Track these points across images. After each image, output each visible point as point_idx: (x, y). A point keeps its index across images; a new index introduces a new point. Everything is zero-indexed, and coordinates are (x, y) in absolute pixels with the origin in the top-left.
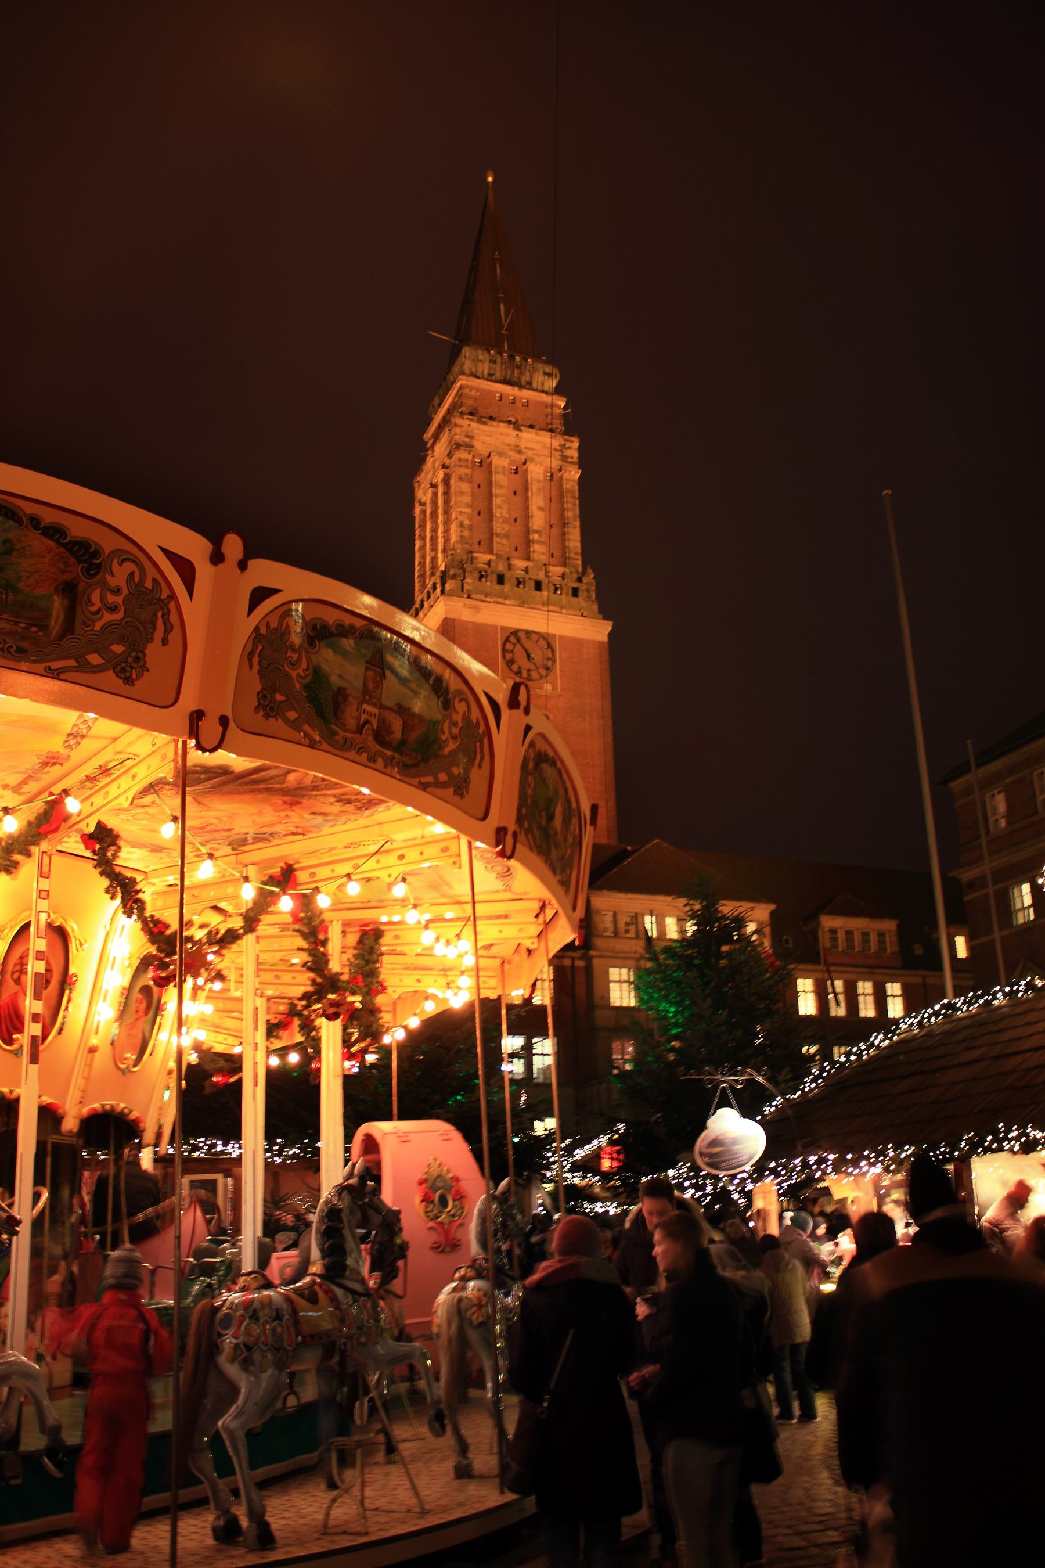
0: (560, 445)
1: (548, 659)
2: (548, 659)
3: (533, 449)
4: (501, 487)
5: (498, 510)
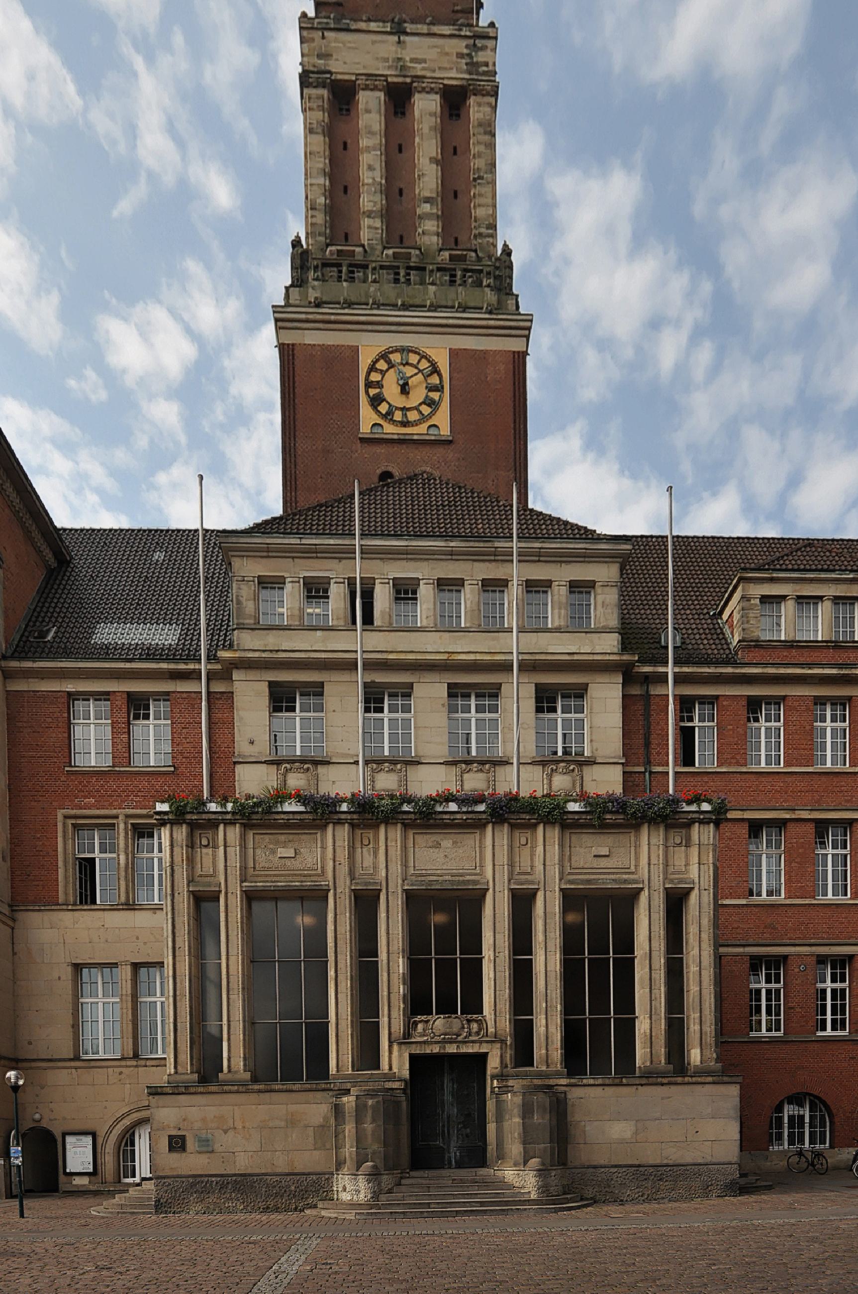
0: (467, 47)
1: (432, 388)
2: (432, 388)
3: (425, 61)
4: (371, 133)
5: (370, 174)
